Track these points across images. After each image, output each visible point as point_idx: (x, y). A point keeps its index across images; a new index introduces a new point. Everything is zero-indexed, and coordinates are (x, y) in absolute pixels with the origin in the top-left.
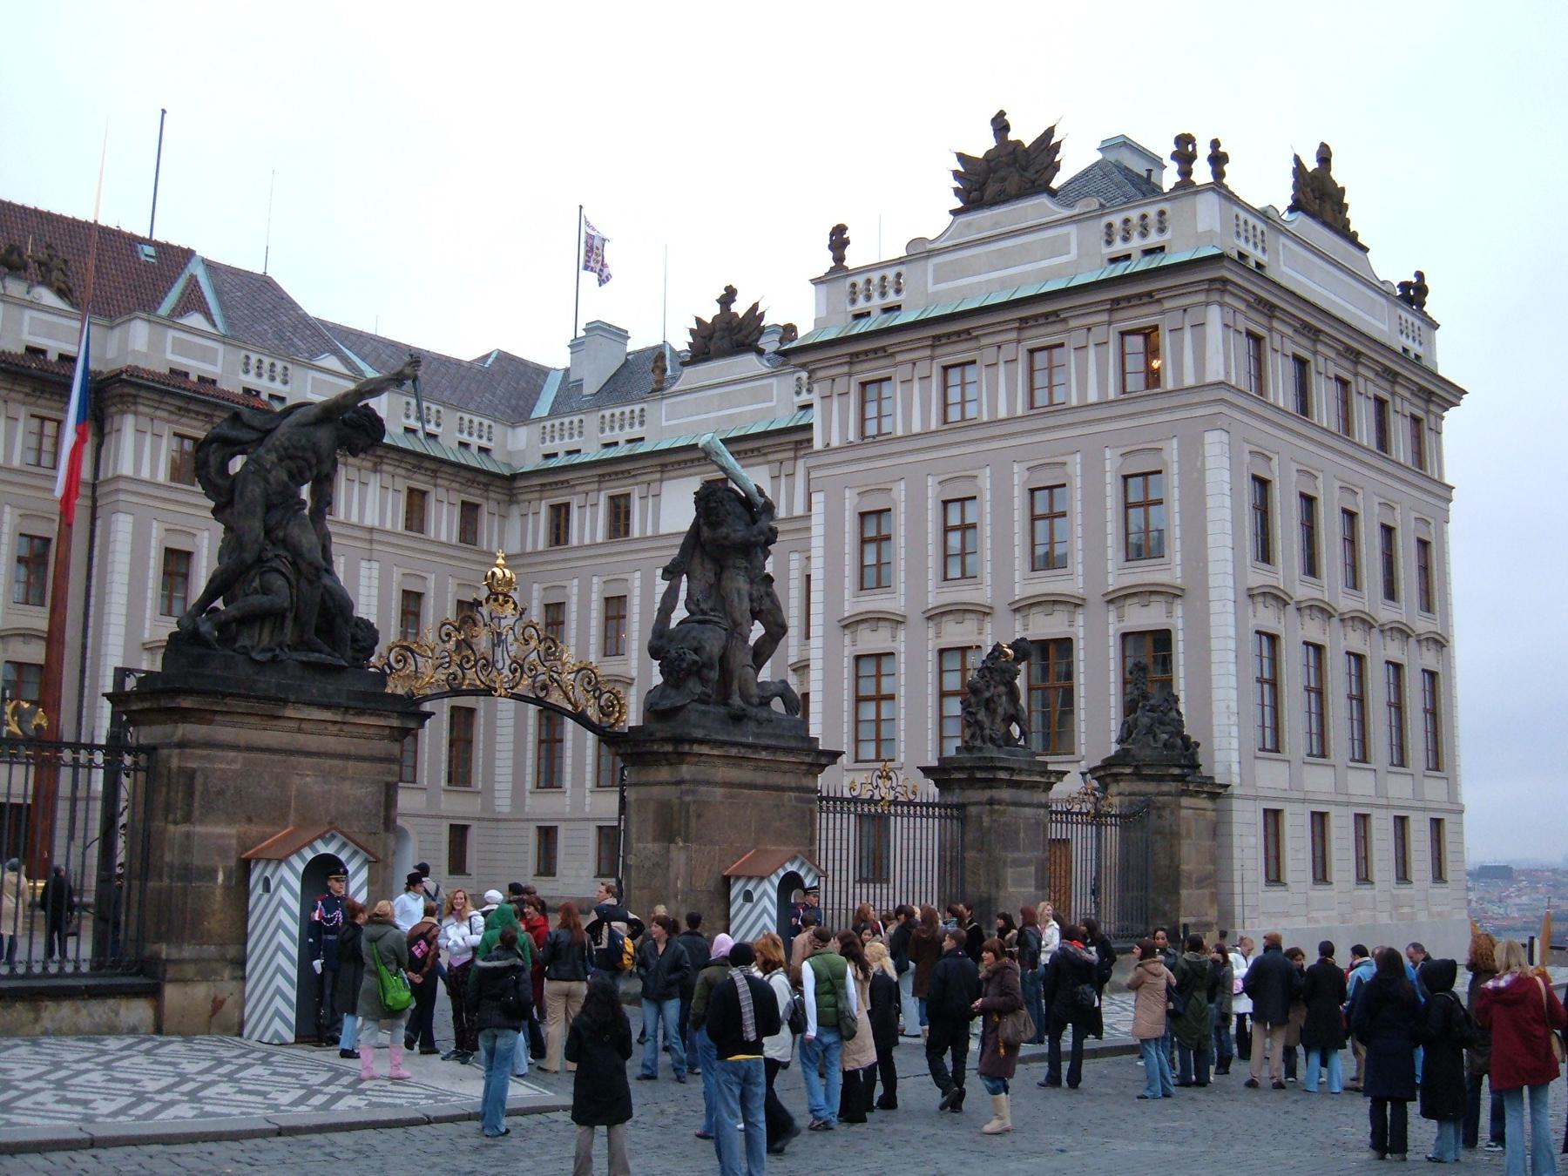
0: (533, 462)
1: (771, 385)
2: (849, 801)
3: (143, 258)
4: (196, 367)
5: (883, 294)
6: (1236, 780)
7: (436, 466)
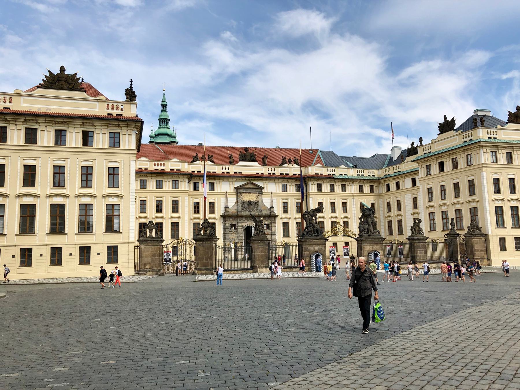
0: (382, 176)
4: (319, 173)
6: (490, 233)
7: (364, 180)
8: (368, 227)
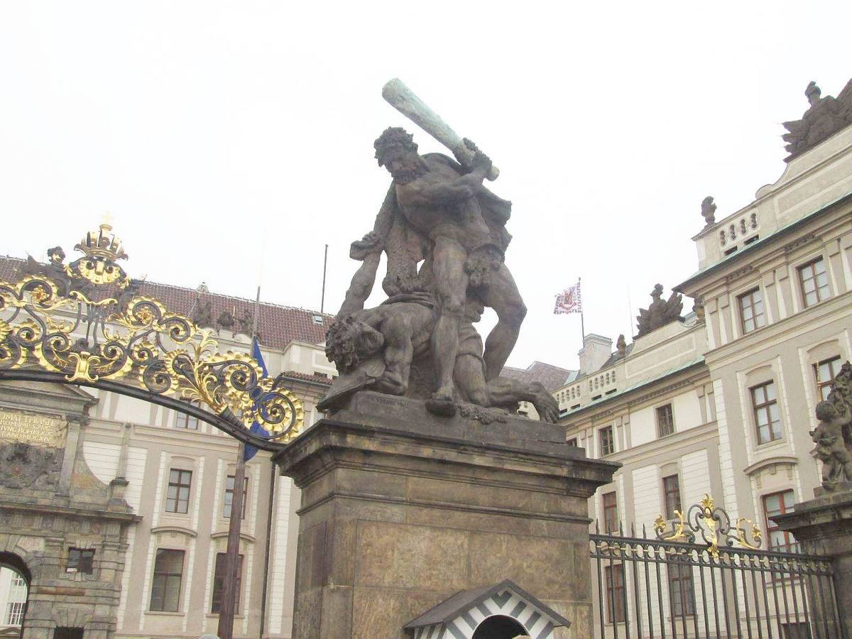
1: (691, 339)
2: (656, 544)
3: (315, 322)
5: (744, 232)
8: (430, 327)
